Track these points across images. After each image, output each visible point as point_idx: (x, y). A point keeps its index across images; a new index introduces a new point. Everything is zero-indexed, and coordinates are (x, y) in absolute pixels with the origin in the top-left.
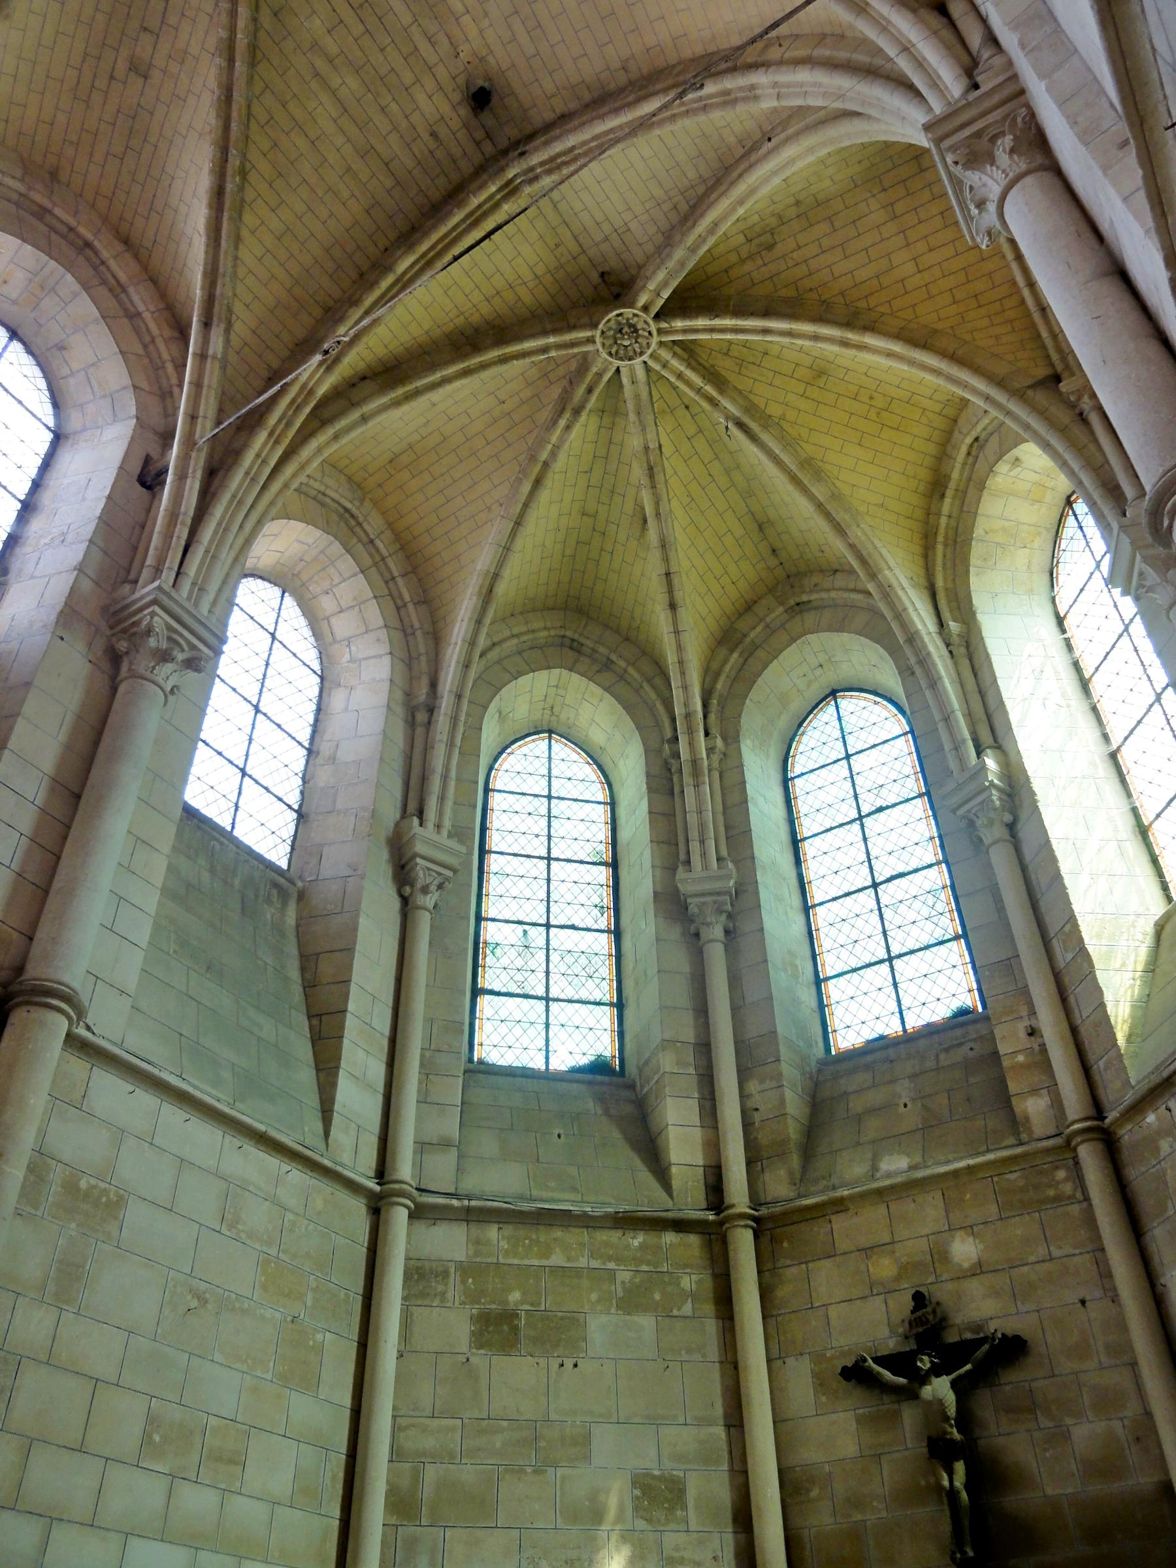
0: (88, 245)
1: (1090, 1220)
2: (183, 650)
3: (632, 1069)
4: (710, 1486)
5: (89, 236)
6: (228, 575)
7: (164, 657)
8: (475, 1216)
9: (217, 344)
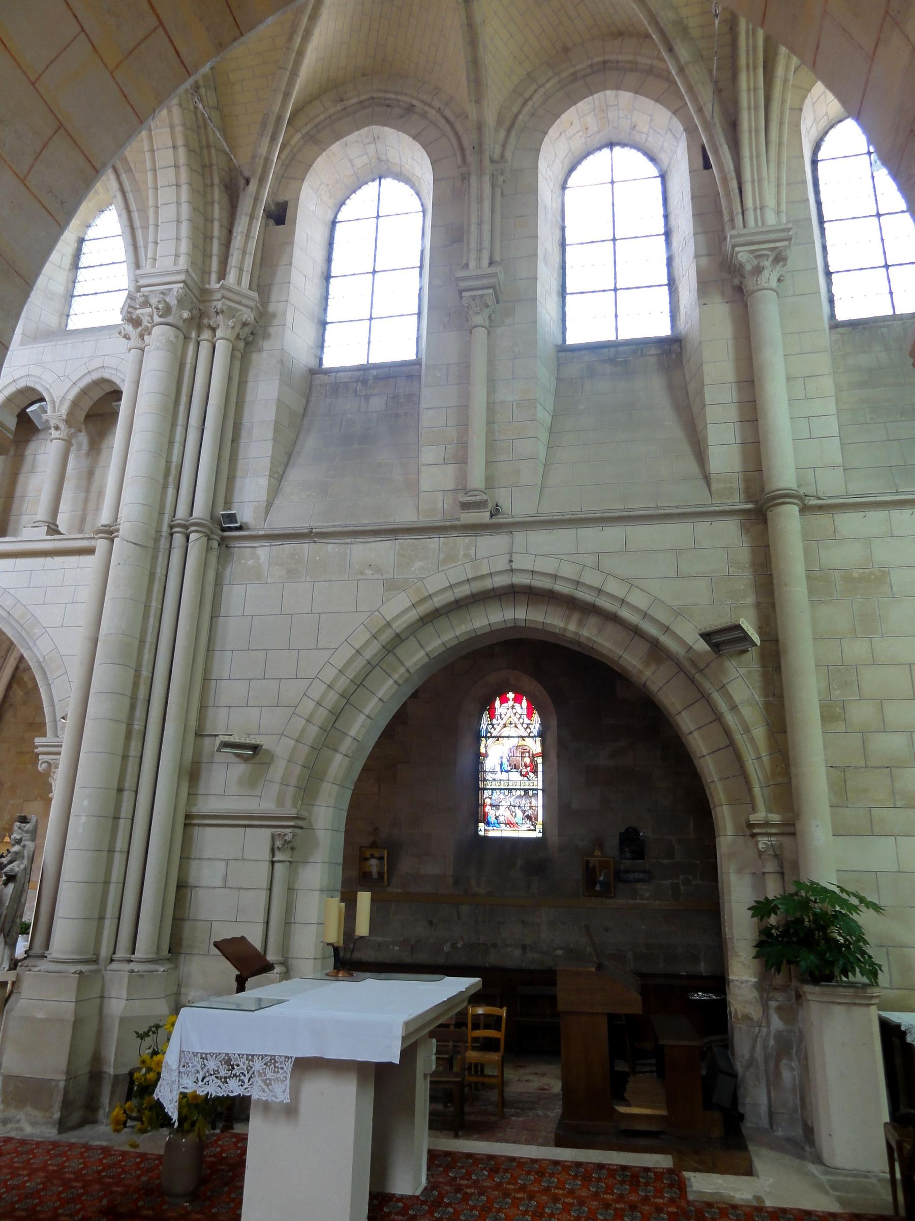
0: (604, 62)
2: (768, 256)
5: (600, 59)
6: (778, 178)
7: (758, 270)
9: (684, 53)
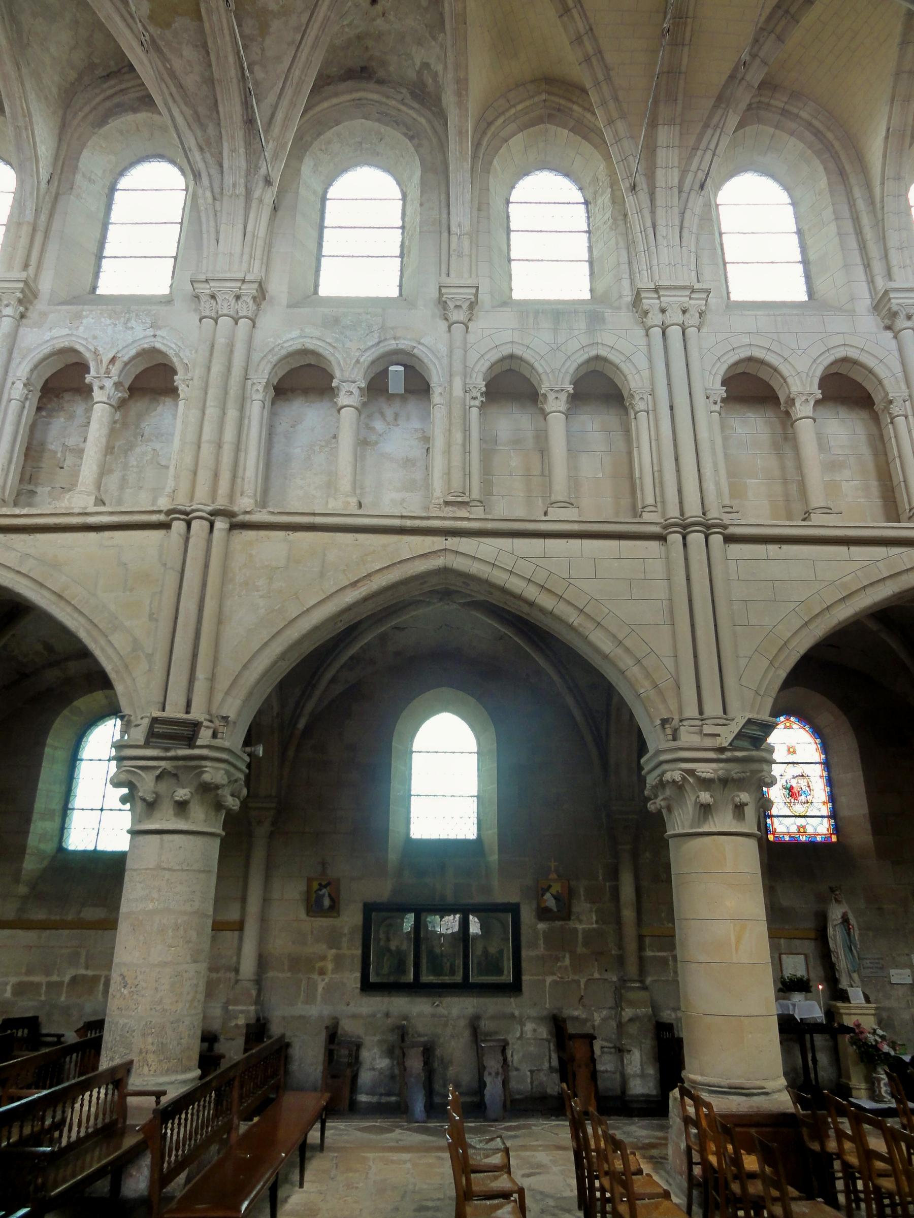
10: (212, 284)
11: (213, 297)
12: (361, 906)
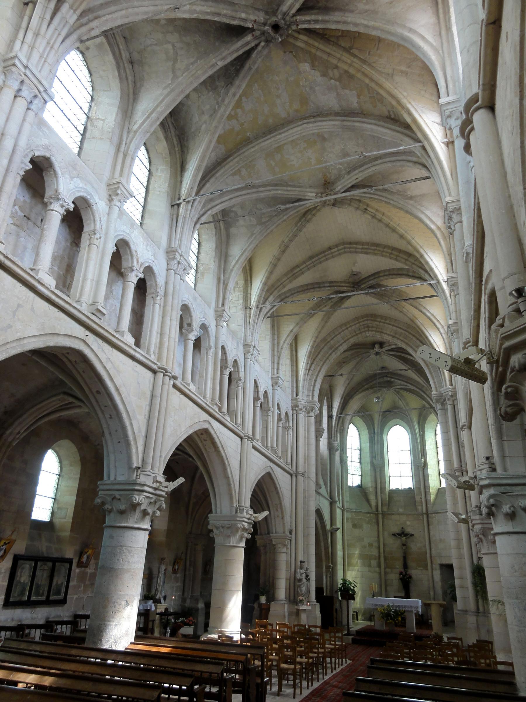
1: (424, 523)
3: (364, 486)
4: (375, 544)
8: (351, 512)
10: (182, 258)
11: (179, 263)
12: (12, 556)
